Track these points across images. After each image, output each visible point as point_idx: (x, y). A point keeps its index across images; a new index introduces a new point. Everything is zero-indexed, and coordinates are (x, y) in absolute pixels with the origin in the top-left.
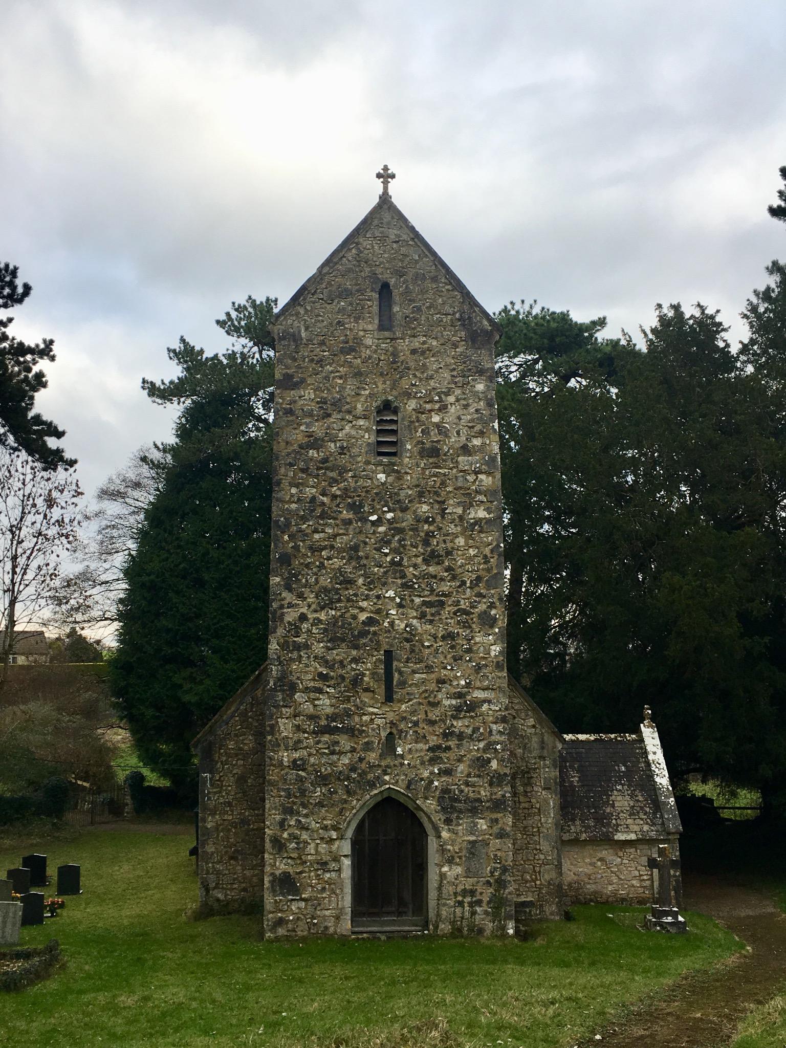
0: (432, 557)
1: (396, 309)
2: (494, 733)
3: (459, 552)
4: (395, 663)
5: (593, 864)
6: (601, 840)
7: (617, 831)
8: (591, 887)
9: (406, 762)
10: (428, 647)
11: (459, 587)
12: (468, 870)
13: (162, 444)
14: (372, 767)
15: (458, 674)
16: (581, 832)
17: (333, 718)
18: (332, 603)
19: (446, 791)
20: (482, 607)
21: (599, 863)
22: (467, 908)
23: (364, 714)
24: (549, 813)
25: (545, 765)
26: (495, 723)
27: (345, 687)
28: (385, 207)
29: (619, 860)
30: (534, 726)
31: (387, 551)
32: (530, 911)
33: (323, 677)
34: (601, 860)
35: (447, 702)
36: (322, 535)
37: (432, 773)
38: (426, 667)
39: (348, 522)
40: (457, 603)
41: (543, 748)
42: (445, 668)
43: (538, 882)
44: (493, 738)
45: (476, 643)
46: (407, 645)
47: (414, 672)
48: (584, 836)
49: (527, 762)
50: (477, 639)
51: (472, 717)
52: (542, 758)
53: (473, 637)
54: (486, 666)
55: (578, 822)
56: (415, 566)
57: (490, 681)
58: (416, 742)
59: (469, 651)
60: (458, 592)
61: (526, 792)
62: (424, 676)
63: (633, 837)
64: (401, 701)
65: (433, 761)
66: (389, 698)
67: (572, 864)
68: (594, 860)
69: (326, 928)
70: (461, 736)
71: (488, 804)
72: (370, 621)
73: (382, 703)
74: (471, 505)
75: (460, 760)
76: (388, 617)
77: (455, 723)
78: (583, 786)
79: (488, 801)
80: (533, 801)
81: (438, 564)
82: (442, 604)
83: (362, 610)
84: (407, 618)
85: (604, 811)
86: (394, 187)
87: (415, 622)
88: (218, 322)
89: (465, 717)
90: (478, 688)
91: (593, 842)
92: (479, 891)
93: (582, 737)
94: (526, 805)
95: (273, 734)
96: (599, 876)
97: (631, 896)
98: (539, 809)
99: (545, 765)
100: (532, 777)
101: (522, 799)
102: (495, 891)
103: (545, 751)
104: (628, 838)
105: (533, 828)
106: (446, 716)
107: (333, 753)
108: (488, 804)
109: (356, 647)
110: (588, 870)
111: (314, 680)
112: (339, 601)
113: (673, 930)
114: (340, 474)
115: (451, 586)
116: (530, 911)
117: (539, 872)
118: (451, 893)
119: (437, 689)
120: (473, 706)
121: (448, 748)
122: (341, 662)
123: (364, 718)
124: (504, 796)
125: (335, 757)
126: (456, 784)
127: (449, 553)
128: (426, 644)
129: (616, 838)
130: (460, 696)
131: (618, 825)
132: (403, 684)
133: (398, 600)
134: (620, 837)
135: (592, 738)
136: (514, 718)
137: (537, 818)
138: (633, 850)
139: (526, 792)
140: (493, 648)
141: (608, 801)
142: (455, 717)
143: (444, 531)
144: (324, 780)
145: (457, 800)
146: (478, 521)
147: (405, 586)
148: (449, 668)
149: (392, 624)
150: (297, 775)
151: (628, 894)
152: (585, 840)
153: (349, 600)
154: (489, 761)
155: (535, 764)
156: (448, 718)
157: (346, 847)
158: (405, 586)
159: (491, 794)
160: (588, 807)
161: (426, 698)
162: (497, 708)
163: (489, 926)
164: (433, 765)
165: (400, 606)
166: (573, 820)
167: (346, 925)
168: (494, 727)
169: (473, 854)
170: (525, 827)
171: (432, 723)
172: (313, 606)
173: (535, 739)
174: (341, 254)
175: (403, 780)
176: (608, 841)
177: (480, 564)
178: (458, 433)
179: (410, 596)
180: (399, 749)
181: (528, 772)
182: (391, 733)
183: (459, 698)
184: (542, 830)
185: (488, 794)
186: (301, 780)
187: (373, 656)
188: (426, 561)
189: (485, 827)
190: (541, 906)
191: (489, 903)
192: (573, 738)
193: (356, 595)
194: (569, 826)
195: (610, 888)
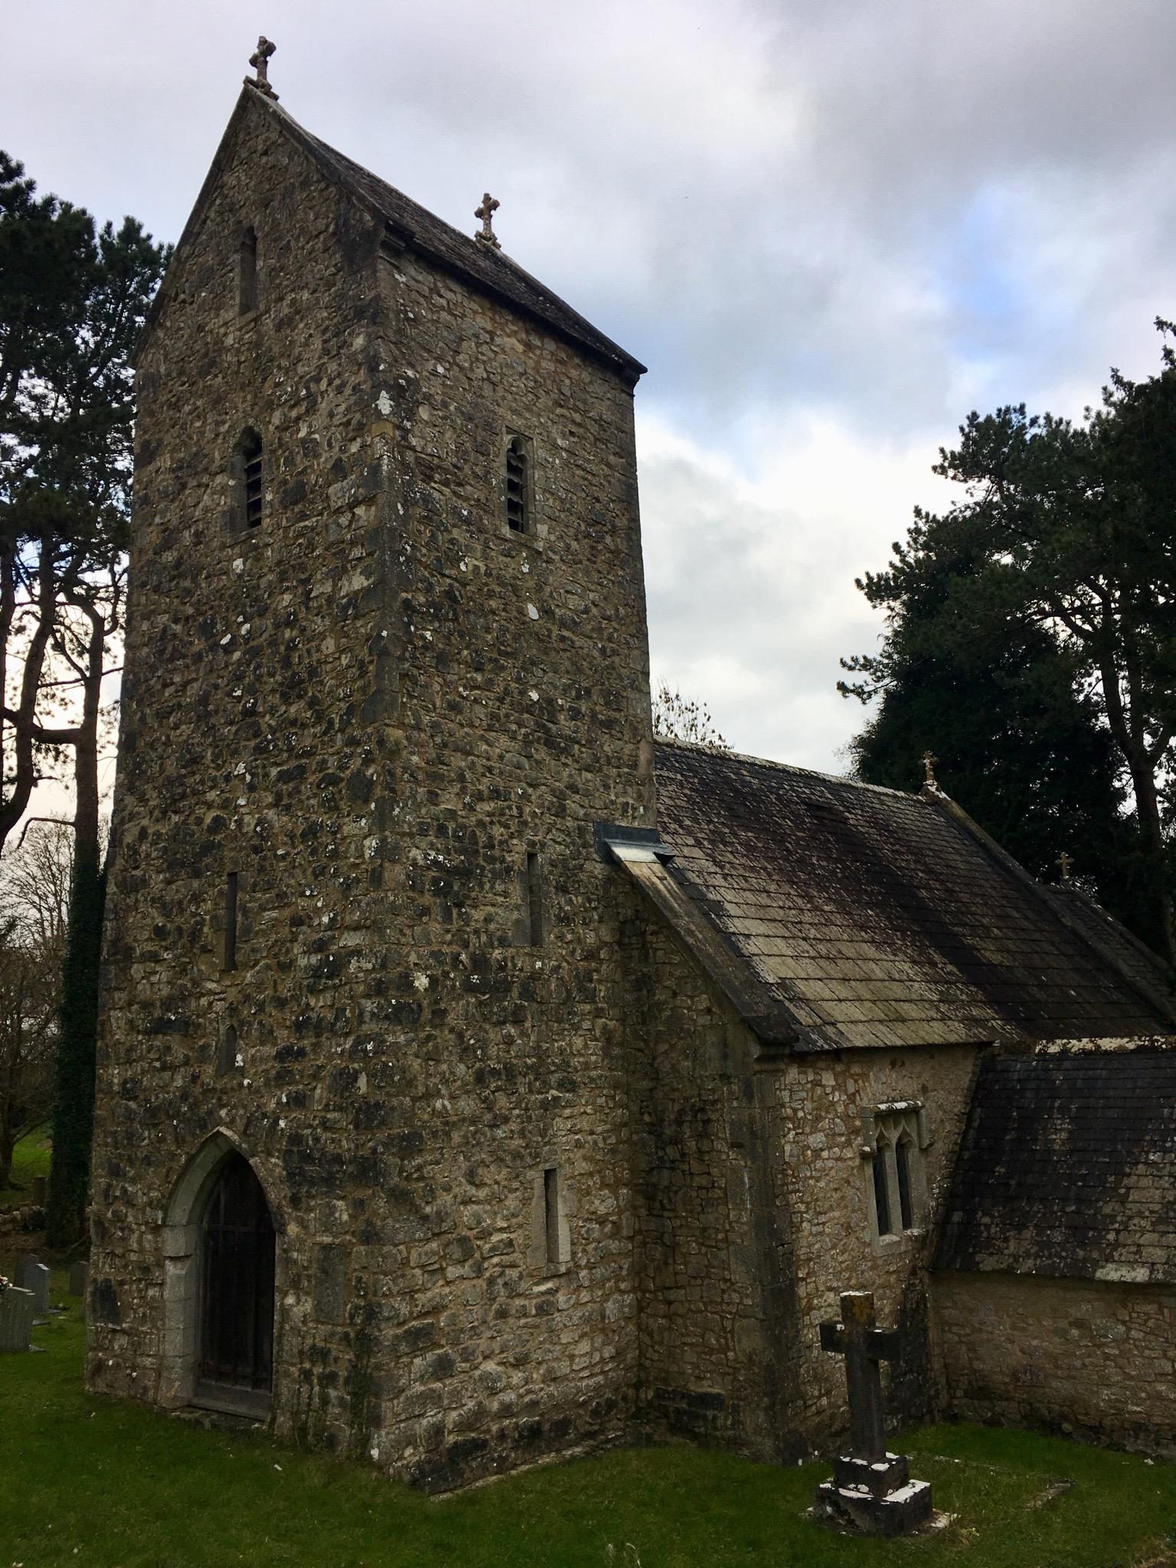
0: (291, 690)
1: (260, 263)
2: (367, 1017)
3: (329, 667)
4: (240, 895)
5: (1063, 1333)
6: (1063, 1277)
7: (1109, 1259)
8: (1060, 1387)
9: (246, 1082)
10: (283, 857)
11: (325, 733)
12: (318, 1307)
13: (865, 658)
14: (208, 1091)
15: (319, 904)
16: (1028, 1255)
17: (168, 1004)
18: (175, 801)
19: (296, 1139)
20: (355, 764)
21: (1075, 1332)
22: (317, 1389)
23: (203, 995)
24: (743, 1201)
25: (731, 1093)
26: (368, 996)
27: (183, 947)
28: (250, 104)
29: (1122, 1328)
30: (709, 1011)
31: (239, 693)
32: (715, 1418)
33: (159, 933)
34: (1079, 1324)
35: (302, 962)
36: (172, 689)
37: (279, 1103)
38: (277, 895)
39: (198, 657)
40: (322, 765)
41: (725, 1057)
42: (302, 894)
43: (731, 1354)
44: (365, 1027)
45: (344, 838)
46: (255, 858)
47: (263, 909)
48: (1028, 1265)
49: (700, 1087)
50: (346, 829)
51: (335, 988)
52: (725, 1078)
53: (340, 827)
54: (357, 880)
55: (1029, 1233)
56: (272, 711)
57: (363, 912)
58: (262, 1044)
59: (335, 855)
60: (323, 743)
61: (700, 1152)
62: (274, 914)
63: (1141, 1275)
64: (247, 966)
65: (282, 1078)
66: (231, 965)
67: (1014, 1328)
68: (1063, 1324)
69: (146, 1389)
70: (319, 1027)
71: (351, 1168)
72: (218, 824)
73: (223, 971)
74: (345, 571)
75: (315, 1077)
76: (236, 813)
77: (312, 1003)
78: (1071, 1152)
79: (351, 1162)
80: (715, 1171)
81: (300, 697)
82: (302, 770)
83: (210, 806)
84: (259, 809)
85: (1098, 1211)
86: (277, 73)
87: (271, 814)
88: (935, 468)
89: (326, 988)
90: (348, 928)
91: (1043, 1278)
92: (334, 1353)
93: (1108, 1044)
94: (704, 1181)
95: (103, 1038)
96: (1078, 1363)
97: (1157, 1420)
98: (725, 1190)
99: (731, 1093)
100: (709, 1121)
101: (696, 1167)
102: (357, 1357)
103: (730, 1063)
104: (1128, 1278)
105: (718, 1231)
106: (300, 989)
107: (163, 1068)
108: (351, 1168)
109: (197, 874)
110: (1053, 1345)
111: (150, 939)
112: (184, 796)
113: (863, 1522)
114: (194, 580)
115: (315, 736)
116: (715, 1418)
117: (732, 1331)
118: (295, 1351)
119: (290, 937)
120: (336, 968)
121: (302, 1053)
122: (180, 902)
123: (204, 1001)
124: (374, 1151)
125: (167, 1075)
126: (311, 1126)
127: (313, 672)
128: (280, 852)
129: (1100, 1274)
130: (320, 946)
131: (1116, 1245)
132: (248, 930)
133: (248, 777)
134: (1111, 1273)
135: (1131, 1046)
136: (675, 995)
137: (722, 1209)
138: (1151, 1308)
139: (700, 1152)
140: (367, 842)
141: (1115, 1189)
142: (313, 990)
143: (308, 632)
144: (154, 1116)
145: (308, 1158)
146: (354, 598)
147: (260, 750)
148: (308, 893)
149: (239, 823)
150: (127, 1108)
151: (1149, 1414)
152: (1028, 1275)
153: (195, 793)
154: (354, 1077)
155: (713, 1090)
156: (304, 992)
157: (175, 1242)
158: (260, 750)
159: (357, 1146)
160: (1065, 1200)
161: (275, 956)
162: (370, 966)
163: (347, 1432)
164: (280, 1087)
165: (252, 788)
166: (1021, 1227)
167: (174, 1388)
168: (369, 1005)
169: (327, 1274)
170: (704, 1230)
171: (281, 1003)
172: (156, 813)
173: (711, 1038)
174: (203, 216)
175: (241, 1117)
176: (1080, 1279)
177: (354, 681)
178: (330, 444)
179: (264, 767)
180: (239, 1057)
181: (702, 1110)
182: (232, 1027)
183: (317, 951)
184: (732, 1236)
185: (352, 1146)
186: (130, 1116)
187: (215, 886)
188: (286, 699)
189: (345, 1217)
190: (736, 1409)
191: (347, 1381)
192: (1090, 1046)
193: (202, 782)
194: (1006, 1240)
195: (1106, 1393)
